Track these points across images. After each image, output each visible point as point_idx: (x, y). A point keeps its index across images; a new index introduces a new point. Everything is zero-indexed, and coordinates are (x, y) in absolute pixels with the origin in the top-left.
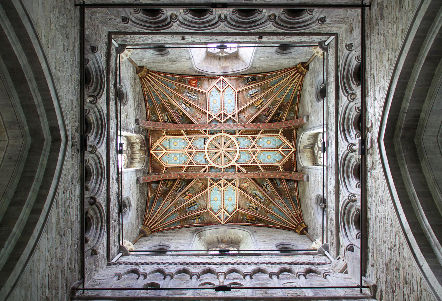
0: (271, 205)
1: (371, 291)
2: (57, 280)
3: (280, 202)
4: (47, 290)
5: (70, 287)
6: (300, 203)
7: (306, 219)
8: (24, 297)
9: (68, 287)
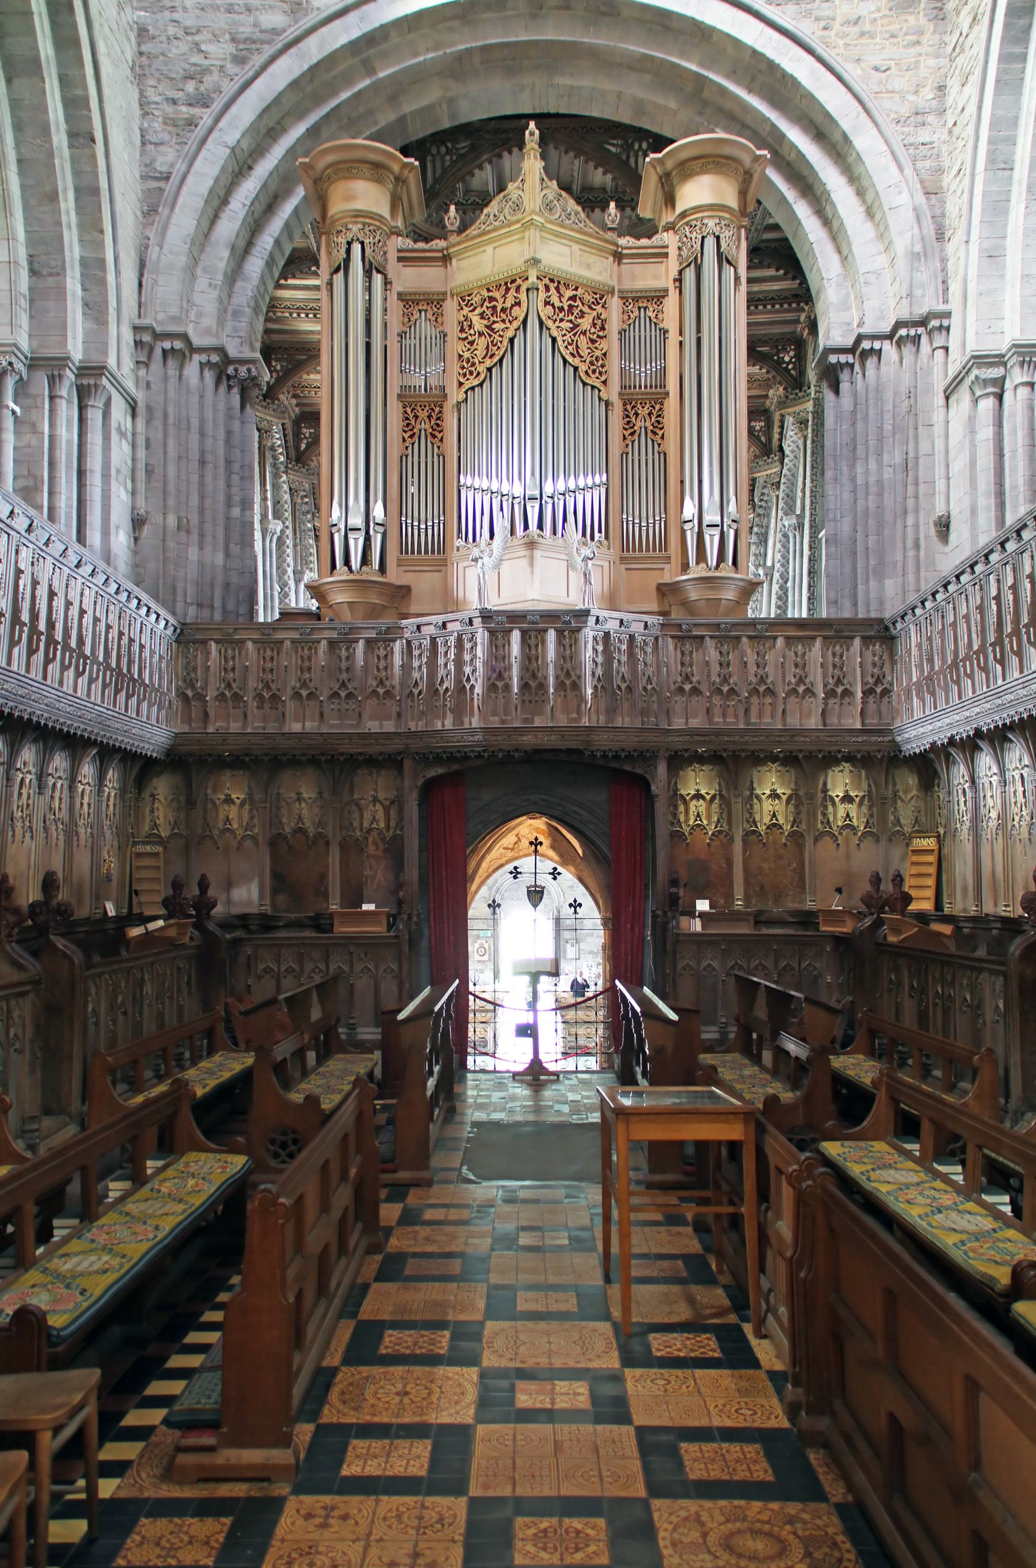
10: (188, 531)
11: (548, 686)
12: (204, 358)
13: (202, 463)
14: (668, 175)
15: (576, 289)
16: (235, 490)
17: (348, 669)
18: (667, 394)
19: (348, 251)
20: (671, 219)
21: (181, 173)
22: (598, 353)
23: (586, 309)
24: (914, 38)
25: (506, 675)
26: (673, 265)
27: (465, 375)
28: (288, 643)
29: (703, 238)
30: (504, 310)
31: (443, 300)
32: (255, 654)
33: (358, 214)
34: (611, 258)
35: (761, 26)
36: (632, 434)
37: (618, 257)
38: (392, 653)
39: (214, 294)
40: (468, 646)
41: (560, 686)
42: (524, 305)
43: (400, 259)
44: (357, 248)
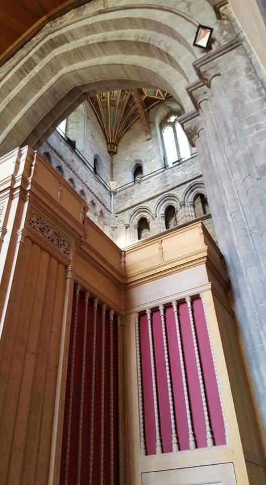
0: (113, 107)
3: (119, 114)
6: (127, 130)
7: (120, 145)
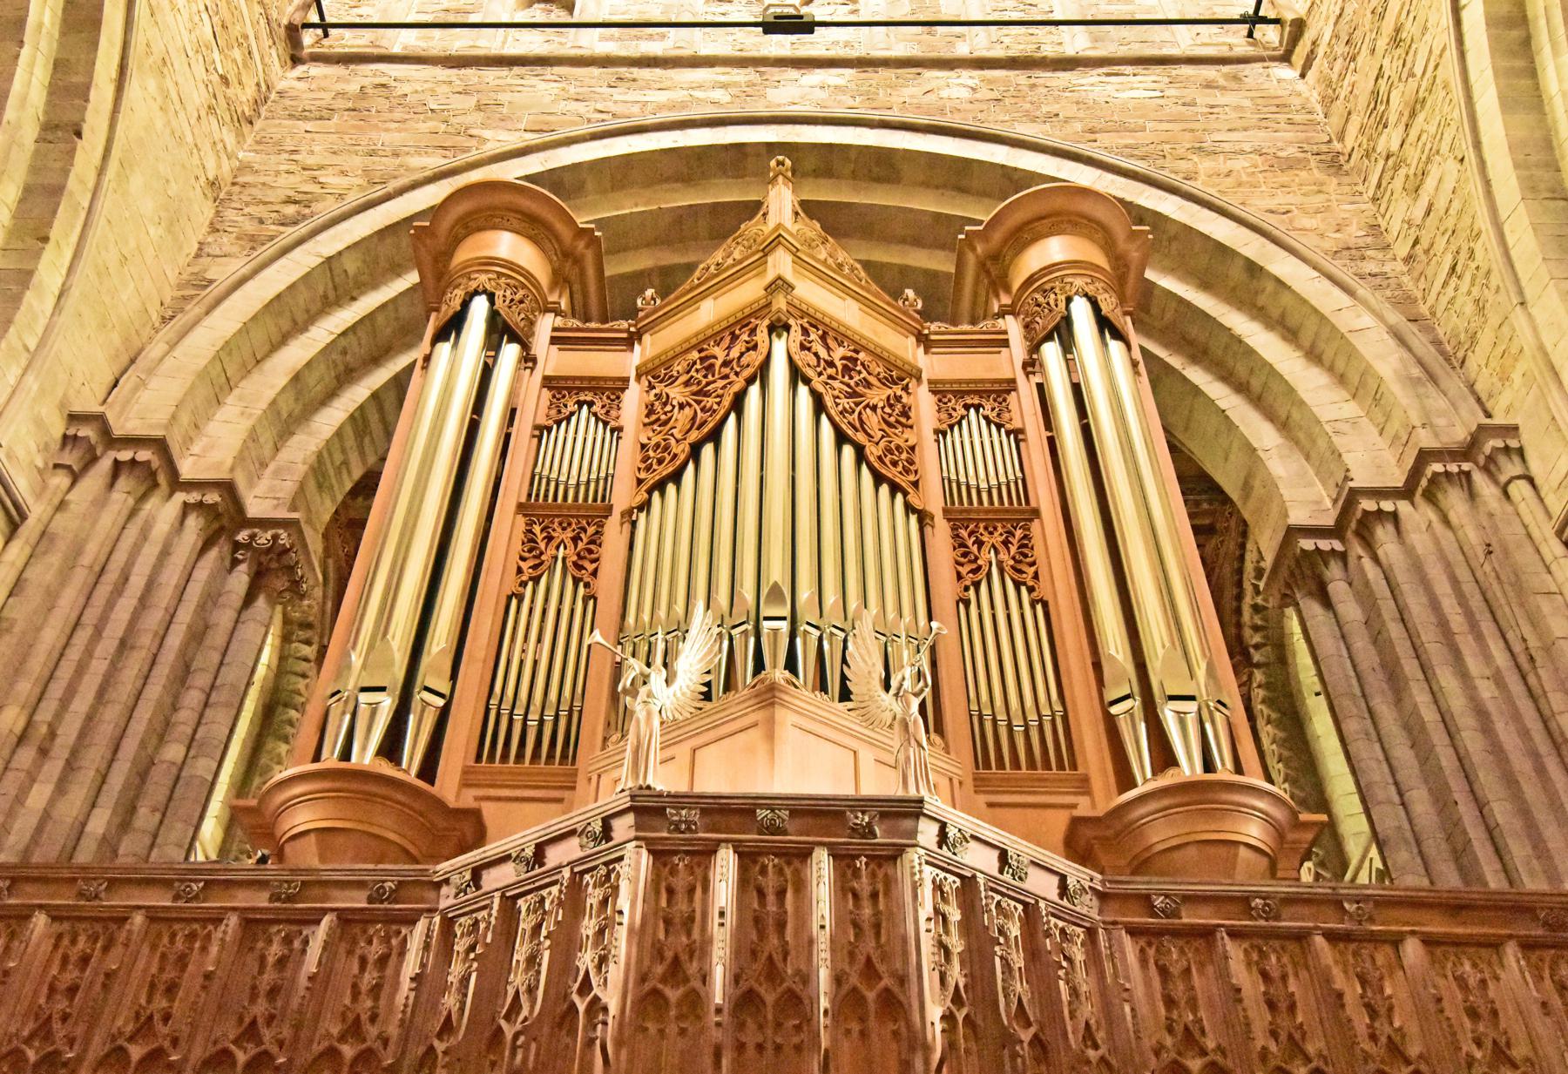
1: (1282, 35)
2: (236, 13)
4: (216, 55)
5: (279, 25)
8: (159, 100)
9: (276, 27)
10: (44, 752)
11: (815, 1000)
12: (193, 497)
13: (125, 645)
14: (996, 257)
15: (857, 352)
16: (186, 716)
17: (273, 992)
18: (1036, 513)
19: (466, 305)
20: (1006, 300)
21: (239, 274)
22: (900, 442)
23: (872, 380)
24: (1315, 188)
25: (693, 968)
26: (1018, 348)
27: (648, 469)
28: (138, 919)
29: (1069, 300)
30: (726, 364)
31: (623, 390)
32: (47, 946)
33: (491, 262)
34: (912, 339)
35: (1099, 172)
36: (976, 571)
37: (924, 341)
38: (402, 952)
39: (245, 425)
40: (594, 897)
41: (848, 1002)
42: (763, 349)
43: (554, 341)
44: (480, 306)
